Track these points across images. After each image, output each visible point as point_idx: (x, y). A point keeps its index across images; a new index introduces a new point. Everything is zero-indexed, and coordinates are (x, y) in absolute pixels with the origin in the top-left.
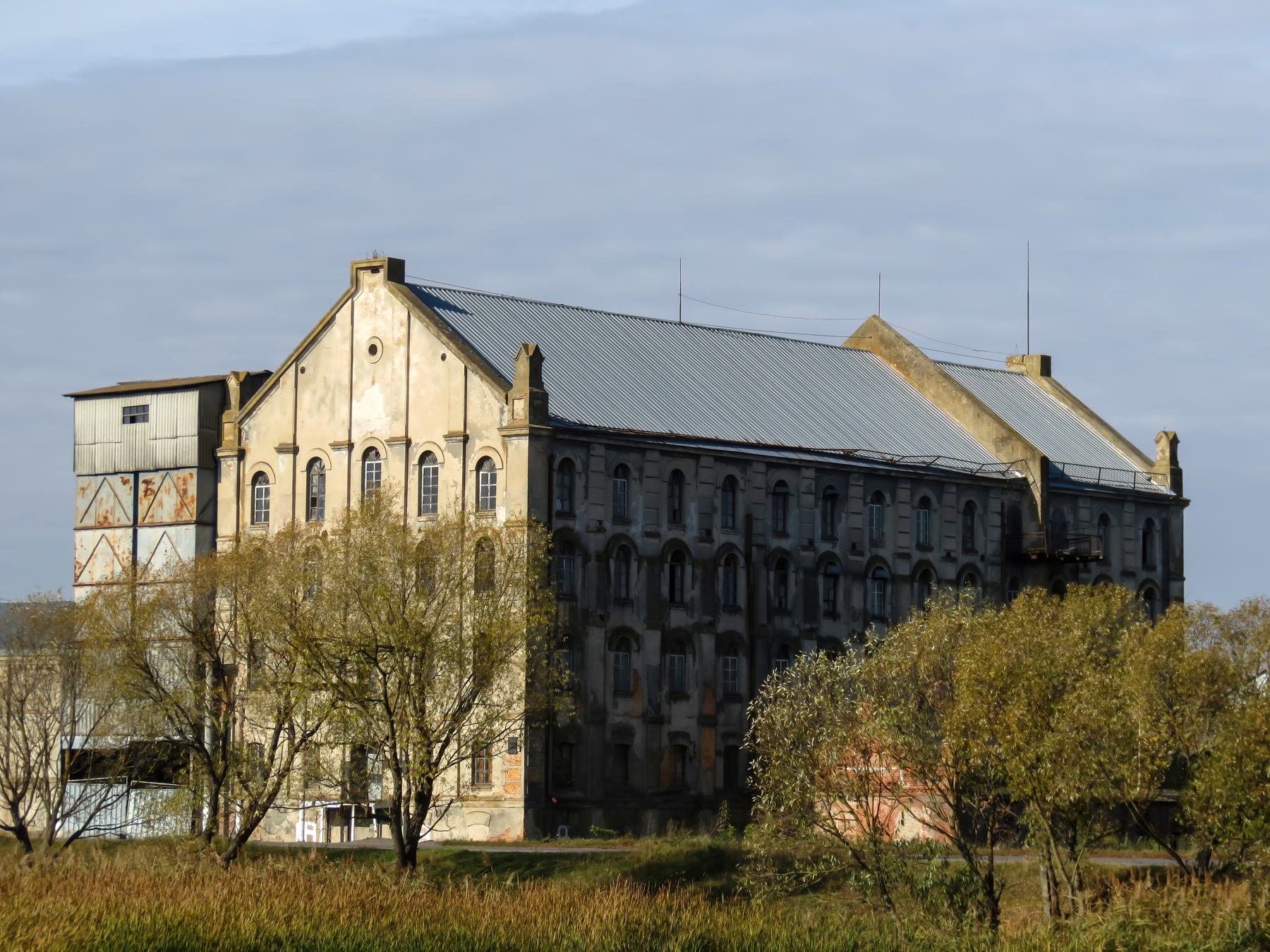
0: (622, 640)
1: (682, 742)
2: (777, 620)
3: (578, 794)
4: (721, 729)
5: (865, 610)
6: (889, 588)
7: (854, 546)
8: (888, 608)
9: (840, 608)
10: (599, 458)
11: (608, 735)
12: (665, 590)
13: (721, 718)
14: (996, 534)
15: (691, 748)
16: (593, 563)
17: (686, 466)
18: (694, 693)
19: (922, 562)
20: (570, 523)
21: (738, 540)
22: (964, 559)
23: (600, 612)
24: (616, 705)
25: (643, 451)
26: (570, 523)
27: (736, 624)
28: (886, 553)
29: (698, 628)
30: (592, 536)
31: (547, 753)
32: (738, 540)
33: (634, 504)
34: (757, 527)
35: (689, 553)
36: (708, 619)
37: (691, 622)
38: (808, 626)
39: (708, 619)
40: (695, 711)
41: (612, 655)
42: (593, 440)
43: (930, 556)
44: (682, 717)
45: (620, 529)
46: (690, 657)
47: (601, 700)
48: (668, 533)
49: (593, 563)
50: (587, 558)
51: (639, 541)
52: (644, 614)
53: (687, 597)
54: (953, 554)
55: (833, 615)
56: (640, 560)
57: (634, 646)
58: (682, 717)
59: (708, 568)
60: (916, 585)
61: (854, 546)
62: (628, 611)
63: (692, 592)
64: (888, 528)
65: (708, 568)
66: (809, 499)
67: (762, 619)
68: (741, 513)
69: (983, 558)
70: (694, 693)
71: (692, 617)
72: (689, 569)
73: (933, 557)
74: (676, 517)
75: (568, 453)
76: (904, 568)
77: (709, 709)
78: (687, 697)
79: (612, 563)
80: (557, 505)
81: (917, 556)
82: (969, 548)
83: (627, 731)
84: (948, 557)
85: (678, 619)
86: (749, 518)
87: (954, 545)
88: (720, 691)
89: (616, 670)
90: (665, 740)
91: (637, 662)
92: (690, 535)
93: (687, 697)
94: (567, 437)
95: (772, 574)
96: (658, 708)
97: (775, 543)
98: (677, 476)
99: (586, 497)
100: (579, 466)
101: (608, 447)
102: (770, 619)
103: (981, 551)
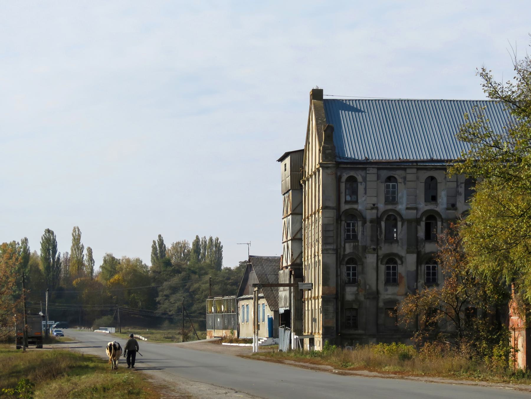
3: (360, 332)
10: (372, 174)
12: (421, 234)
16: (368, 224)
20: (355, 206)
23: (373, 247)
24: (386, 290)
25: (405, 169)
26: (355, 206)
30: (368, 211)
33: (400, 195)
42: (367, 166)
48: (424, 207)
49: (368, 224)
50: (364, 222)
51: (404, 212)
52: (405, 247)
56: (403, 220)
57: (399, 262)
62: (395, 246)
75: (352, 173)
79: (383, 224)
85: (429, 247)
89: (388, 274)
94: (349, 166)
99: (366, 193)
100: (360, 179)
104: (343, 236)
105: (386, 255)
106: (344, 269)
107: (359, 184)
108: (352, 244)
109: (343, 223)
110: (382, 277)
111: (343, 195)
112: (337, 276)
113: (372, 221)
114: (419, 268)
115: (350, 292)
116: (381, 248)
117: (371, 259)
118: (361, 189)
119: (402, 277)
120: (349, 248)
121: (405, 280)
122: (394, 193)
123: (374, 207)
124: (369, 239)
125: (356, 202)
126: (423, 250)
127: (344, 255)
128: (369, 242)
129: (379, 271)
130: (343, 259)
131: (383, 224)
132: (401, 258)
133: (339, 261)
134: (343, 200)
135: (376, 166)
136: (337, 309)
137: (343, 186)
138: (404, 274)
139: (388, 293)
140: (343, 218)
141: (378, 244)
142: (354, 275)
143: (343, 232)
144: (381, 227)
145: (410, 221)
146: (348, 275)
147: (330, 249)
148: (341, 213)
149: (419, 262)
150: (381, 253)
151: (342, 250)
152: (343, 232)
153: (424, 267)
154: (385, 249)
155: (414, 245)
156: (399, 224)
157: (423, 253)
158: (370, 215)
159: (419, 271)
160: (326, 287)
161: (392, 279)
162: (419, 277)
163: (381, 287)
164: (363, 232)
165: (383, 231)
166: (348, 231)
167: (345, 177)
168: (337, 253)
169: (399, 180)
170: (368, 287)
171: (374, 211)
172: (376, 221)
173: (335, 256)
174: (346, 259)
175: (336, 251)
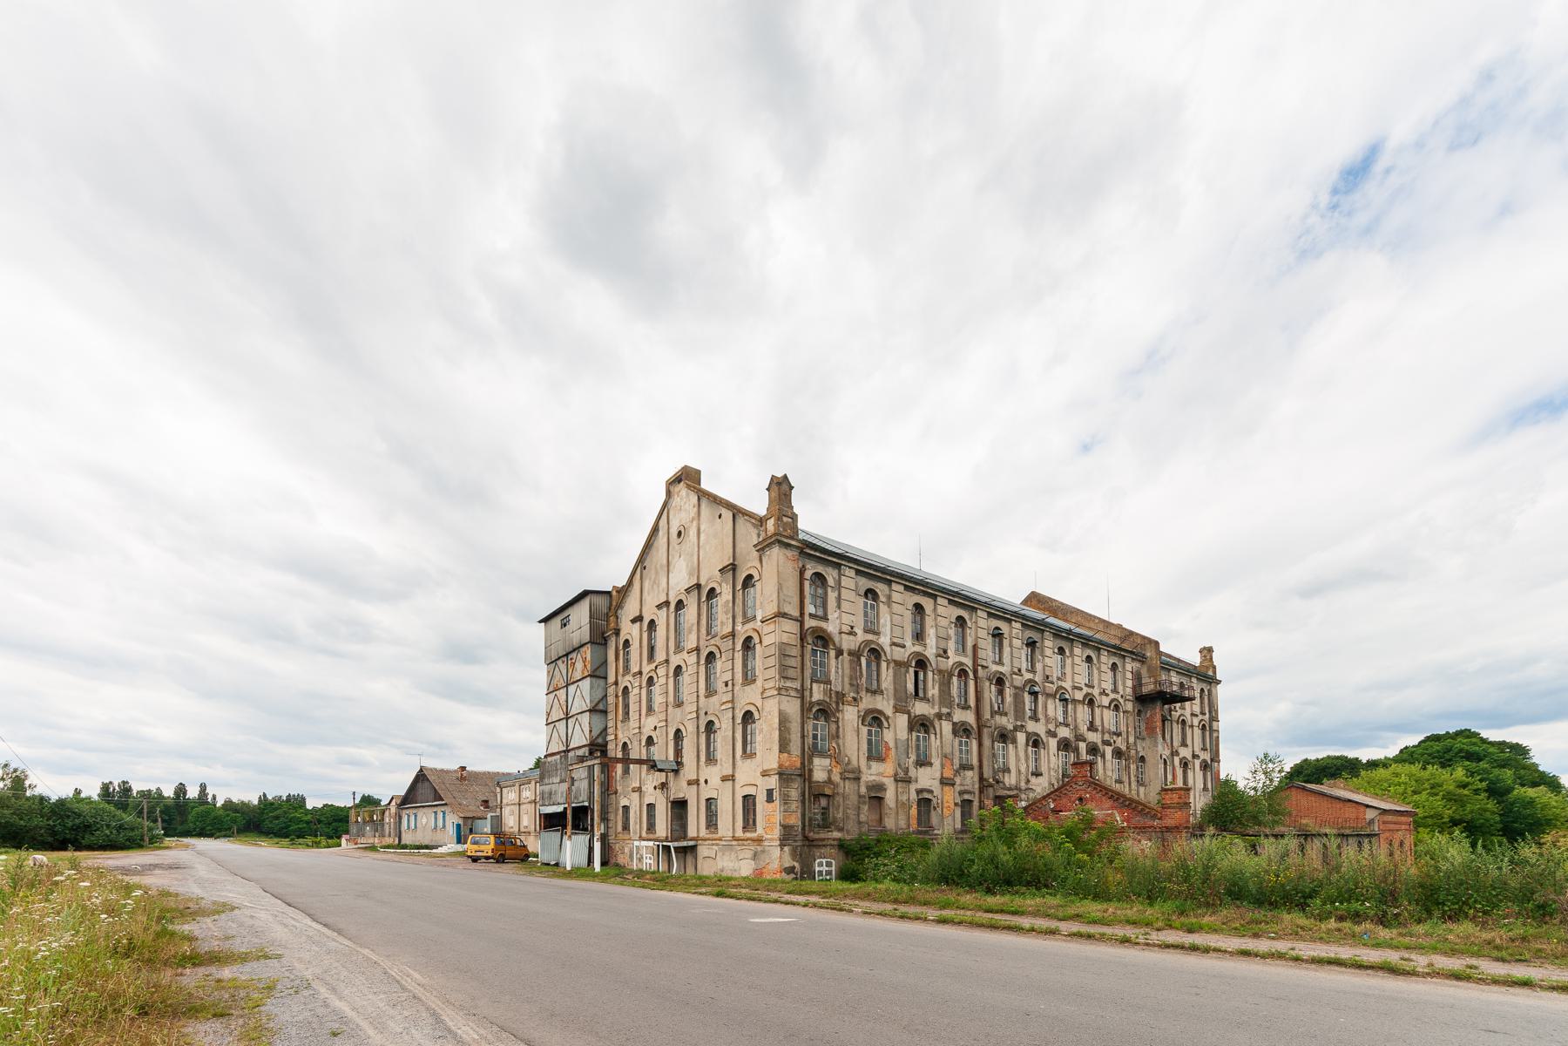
0: (875, 719)
1: (926, 795)
4: (958, 788)
9: (1041, 716)
11: (863, 790)
12: (911, 687)
13: (958, 780)
14: (1129, 683)
17: (927, 603)
18: (937, 762)
19: (1088, 694)
20: (823, 624)
21: (968, 661)
22: (1112, 696)
25: (889, 582)
26: (823, 624)
27: (969, 717)
29: (939, 716)
31: (803, 802)
32: (968, 661)
34: (981, 654)
36: (945, 710)
39: (945, 710)
40: (938, 775)
41: (864, 730)
44: (927, 778)
47: (854, 763)
50: (839, 653)
51: (887, 649)
52: (892, 702)
53: (930, 694)
55: (1035, 718)
58: (927, 778)
59: (945, 677)
62: (879, 698)
63: (933, 691)
65: (945, 677)
66: (1017, 643)
67: (987, 715)
68: (970, 643)
70: (937, 762)
72: (930, 674)
73: (1096, 692)
74: (919, 636)
75: (820, 569)
76: (1079, 696)
77: (948, 773)
78: (931, 764)
80: (810, 609)
81: (1085, 690)
83: (880, 787)
84: (1103, 693)
85: (920, 708)
86: (975, 647)
87: (1108, 686)
88: (957, 762)
89: (870, 742)
90: (913, 796)
91: (888, 736)
92: (930, 652)
93: (931, 764)
96: (907, 771)
98: (918, 608)
100: (831, 582)
101: (858, 572)
102: (993, 713)
105: (868, 712)
113: (850, 653)
117: (850, 715)
119: (888, 749)
121: (893, 753)
125: (825, 618)
127: (812, 704)
132: (887, 719)
133: (805, 708)
137: (807, 584)
145: (898, 664)
154: (868, 702)
158: (848, 643)
164: (838, 671)
167: (808, 574)
168: (802, 698)
169: (882, 598)
172: (855, 655)
173: (798, 701)
175: (801, 694)
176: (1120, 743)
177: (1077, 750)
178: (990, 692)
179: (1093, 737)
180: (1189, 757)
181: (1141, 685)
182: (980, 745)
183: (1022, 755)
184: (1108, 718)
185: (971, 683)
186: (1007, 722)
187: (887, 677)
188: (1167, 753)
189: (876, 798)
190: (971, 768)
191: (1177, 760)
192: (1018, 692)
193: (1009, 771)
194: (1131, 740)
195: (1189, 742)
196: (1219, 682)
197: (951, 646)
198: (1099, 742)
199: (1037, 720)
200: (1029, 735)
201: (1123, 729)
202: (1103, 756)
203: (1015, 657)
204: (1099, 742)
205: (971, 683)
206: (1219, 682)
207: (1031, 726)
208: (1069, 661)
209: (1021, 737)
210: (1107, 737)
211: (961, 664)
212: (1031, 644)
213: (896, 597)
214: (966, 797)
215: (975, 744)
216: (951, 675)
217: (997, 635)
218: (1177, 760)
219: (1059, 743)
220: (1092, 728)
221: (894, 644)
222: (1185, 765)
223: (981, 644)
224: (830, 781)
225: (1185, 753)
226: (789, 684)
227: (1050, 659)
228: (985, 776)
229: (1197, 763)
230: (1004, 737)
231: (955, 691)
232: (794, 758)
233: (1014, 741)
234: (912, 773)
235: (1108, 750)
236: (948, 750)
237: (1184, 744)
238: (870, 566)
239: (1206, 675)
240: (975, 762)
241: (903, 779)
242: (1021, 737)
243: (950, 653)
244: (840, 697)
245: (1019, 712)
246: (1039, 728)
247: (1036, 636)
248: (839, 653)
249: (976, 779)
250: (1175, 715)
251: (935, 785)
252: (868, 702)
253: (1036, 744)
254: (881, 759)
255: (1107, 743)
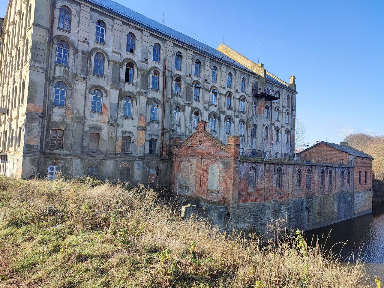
1: (127, 134)
2: (175, 98)
4: (148, 132)
5: (209, 102)
6: (218, 96)
7: (206, 80)
8: (217, 103)
9: (201, 99)
11: (87, 129)
12: (123, 76)
13: (149, 128)
14: (251, 88)
15: (133, 137)
16: (80, 55)
18: (136, 118)
19: (228, 91)
20: (68, 35)
21: (160, 66)
22: (242, 94)
23: (82, 76)
24: (92, 117)
28: (217, 85)
29: (139, 93)
32: (160, 66)
34: (168, 64)
35: (137, 66)
36: (144, 91)
37: (136, 91)
38: (187, 102)
39: (144, 91)
40: (137, 125)
42: (82, 2)
43: (231, 90)
44: (129, 125)
45: (99, 46)
46: (135, 104)
47: (82, 113)
48: (127, 55)
49: (80, 55)
50: (76, 51)
51: (110, 54)
52: (110, 83)
53: (135, 81)
54: (238, 91)
56: (109, 61)
57: (104, 94)
60: (227, 97)
61: (206, 80)
64: (218, 79)
66: (190, 61)
67: (169, 95)
68: (162, 57)
69: (247, 94)
70: (136, 118)
71: (136, 89)
72: (136, 71)
73: (233, 91)
77: (143, 124)
78: (132, 118)
79: (93, 58)
81: (227, 89)
82: (243, 91)
83: (100, 128)
85: (128, 88)
86: (165, 60)
87: (239, 88)
88: (148, 120)
89: (94, 103)
90: (120, 134)
91: (106, 101)
92: (137, 58)
93: (132, 118)
95: (174, 82)
97: (176, 72)
99: (78, 27)
100: (74, 12)
102: (172, 97)
103: (247, 93)
104: (54, 59)
106: (52, 90)
107: (73, 16)
108: (63, 68)
109: (55, 46)
110: (89, 105)
111: (56, 21)
112: (45, 96)
113: (83, 53)
114: (120, 102)
115: (57, 114)
116: (89, 79)
117: (80, 87)
118: (74, 21)
119: (105, 108)
120: (59, 72)
122: (102, 36)
123: (85, 41)
124: (79, 67)
125: (69, 32)
126: (123, 89)
128: (79, 72)
129: (87, 99)
130: (53, 81)
131: (93, 58)
132: (106, 91)
133: (49, 81)
134: (56, 25)
135: (90, 6)
136: (43, 128)
137: (57, 13)
138: (108, 105)
139: (93, 120)
140: (55, 41)
141: (87, 75)
142: (62, 98)
143: (54, 55)
144: (90, 60)
145: (115, 63)
146: (57, 97)
147: (40, 68)
148: (53, 37)
149: (120, 98)
150: (89, 83)
151: (52, 71)
152: (54, 55)
153: (123, 102)
154: (93, 81)
155: (116, 82)
156: (106, 62)
157: (123, 91)
158: (82, 47)
159: (120, 105)
160: (32, 105)
161: (96, 109)
162: (119, 110)
163: (88, 114)
164: (75, 62)
165: (93, 65)
166: (60, 55)
168: (47, 73)
169: (108, 26)
170: (76, 111)
171: (86, 45)
172: (87, 55)
174: (56, 81)
175: (46, 72)
176: (244, 117)
177: (219, 118)
178: (172, 84)
179: (229, 113)
180: (280, 127)
181: (257, 89)
182: (164, 111)
183: (188, 117)
184: (237, 104)
185: (161, 79)
186: (181, 100)
187: (108, 69)
188: (268, 124)
189: (96, 133)
190: (157, 122)
191: (273, 128)
192: (189, 86)
193: (180, 125)
194: (250, 116)
195: (280, 119)
196: (297, 93)
197: (150, 58)
198: (233, 115)
199: (198, 101)
200: (193, 109)
201: (246, 110)
202: (234, 123)
203: (188, 67)
204: (233, 115)
205: (161, 79)
206: (297, 93)
207: (195, 104)
208: (219, 74)
209: (188, 109)
210: (237, 113)
211: (156, 68)
212: (198, 62)
213: (116, 27)
214: (153, 137)
215: (160, 110)
216: (149, 72)
217: (179, 56)
218: (273, 128)
219: (210, 115)
220: (229, 108)
221: (113, 52)
222: (277, 130)
223: (168, 59)
224: (63, 122)
225: (278, 124)
226: (37, 64)
227: (207, 70)
228: (165, 127)
229: (284, 130)
230: (179, 108)
231: (150, 81)
232: (39, 107)
233: (184, 111)
234: (120, 121)
235: (237, 120)
236: (143, 111)
237: (278, 120)
238: (101, 7)
239: (292, 90)
240: (160, 119)
241: (114, 124)
242: (188, 109)
243: (149, 61)
244: (75, 76)
245: (189, 96)
246: (199, 106)
247: (201, 59)
248: (76, 51)
249: (160, 128)
250: (274, 106)
251: (134, 130)
252: (93, 81)
253: (197, 114)
254: (100, 112)
255: (237, 116)
